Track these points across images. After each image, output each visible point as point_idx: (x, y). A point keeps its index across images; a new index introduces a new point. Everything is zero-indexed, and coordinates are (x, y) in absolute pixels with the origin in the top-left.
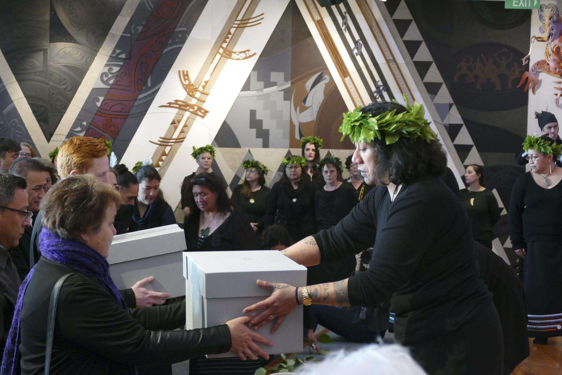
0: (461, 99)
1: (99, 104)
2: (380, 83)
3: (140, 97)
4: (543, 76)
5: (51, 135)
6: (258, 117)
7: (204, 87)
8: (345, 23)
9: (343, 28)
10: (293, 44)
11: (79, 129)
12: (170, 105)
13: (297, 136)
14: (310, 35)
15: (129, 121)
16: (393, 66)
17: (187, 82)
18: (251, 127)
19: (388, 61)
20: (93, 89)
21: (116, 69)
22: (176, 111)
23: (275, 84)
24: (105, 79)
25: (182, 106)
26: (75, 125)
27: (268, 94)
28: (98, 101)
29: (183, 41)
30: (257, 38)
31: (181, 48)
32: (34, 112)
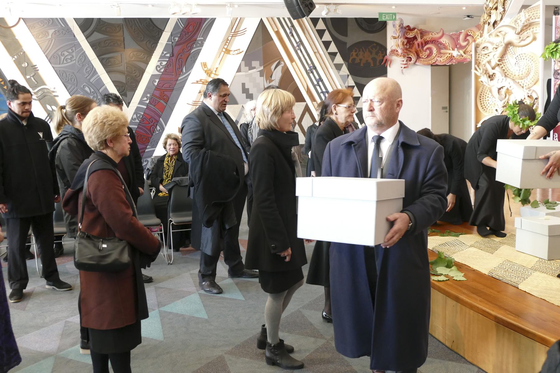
1: (156, 84)
2: (311, 65)
3: (180, 78)
4: (394, 58)
5: (129, 103)
6: (246, 87)
8: (291, 33)
9: (290, 35)
10: (263, 45)
11: (145, 99)
14: (272, 39)
15: (174, 92)
16: (318, 55)
17: (206, 69)
18: (243, 93)
19: (315, 53)
21: (164, 63)
23: (254, 68)
24: (159, 69)
26: (143, 97)
28: (155, 82)
29: (202, 45)
30: (242, 43)
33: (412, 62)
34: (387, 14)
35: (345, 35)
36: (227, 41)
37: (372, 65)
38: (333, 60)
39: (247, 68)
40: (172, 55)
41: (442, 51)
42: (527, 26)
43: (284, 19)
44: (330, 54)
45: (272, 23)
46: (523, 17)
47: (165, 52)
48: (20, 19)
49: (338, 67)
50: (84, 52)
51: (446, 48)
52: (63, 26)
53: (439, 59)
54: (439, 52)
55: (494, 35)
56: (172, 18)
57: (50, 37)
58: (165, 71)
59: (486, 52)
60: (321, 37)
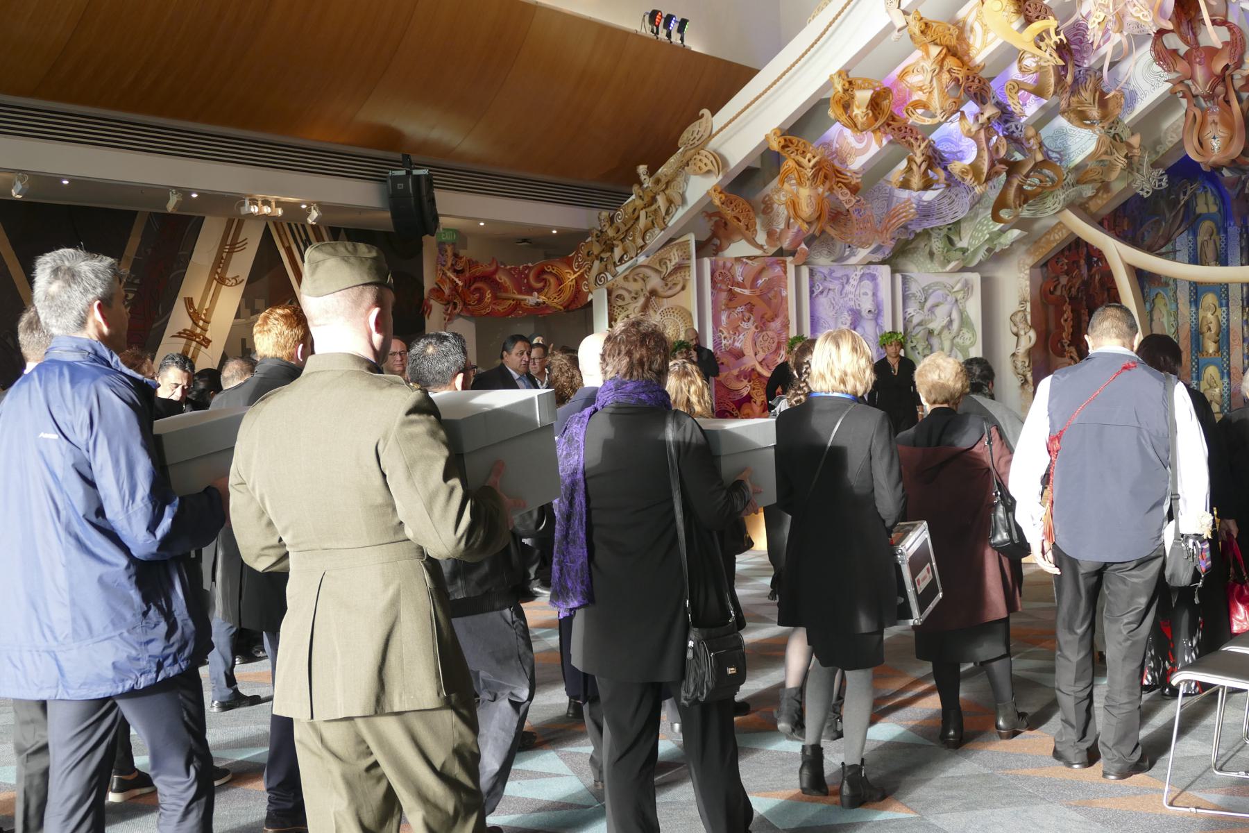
12: (179, 335)
21: (131, 296)
22: (184, 341)
25: (189, 335)
30: (243, 263)
33: (458, 310)
42: (680, 268)
46: (675, 258)
53: (496, 308)
54: (495, 297)
55: (630, 278)
59: (620, 303)
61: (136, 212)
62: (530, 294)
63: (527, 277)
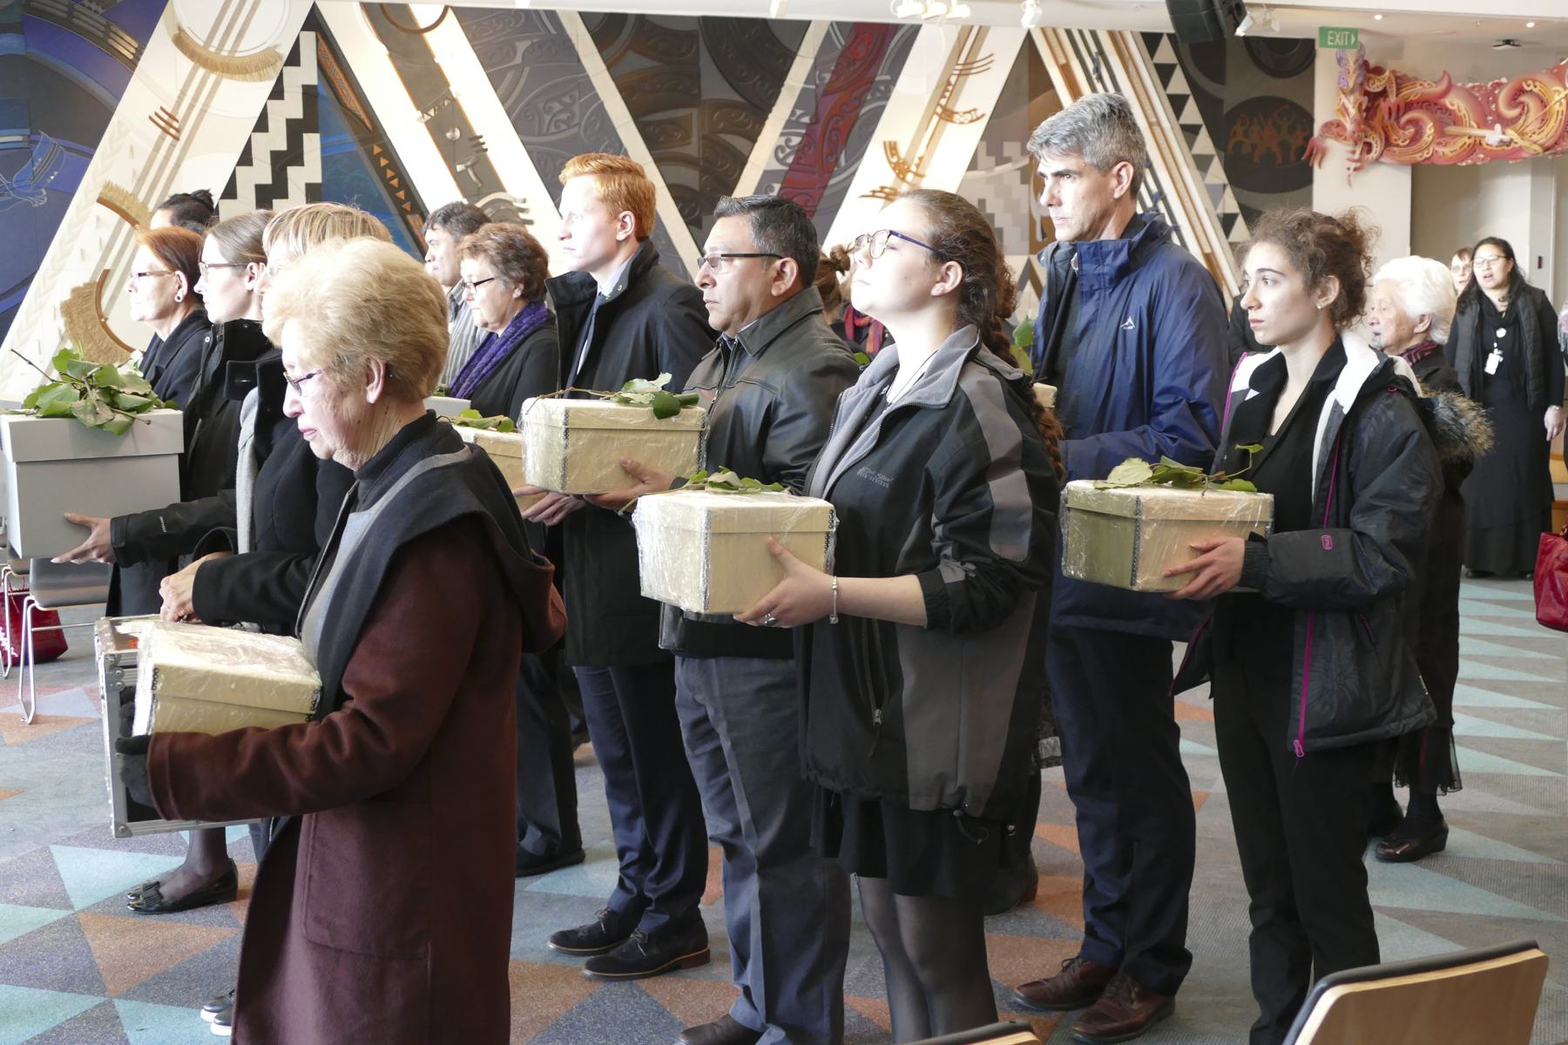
0: (1238, 175)
3: (832, 182)
4: (1330, 143)
7: (918, 166)
8: (1097, 70)
9: (1094, 77)
12: (874, 194)
13: (1039, 237)
14: (1050, 86)
16: (1157, 129)
19: (1150, 125)
20: (766, 172)
21: (796, 141)
23: (1008, 160)
24: (781, 156)
27: (1000, 176)
29: (886, 96)
30: (983, 92)
31: (884, 107)
32: (681, 211)
33: (1373, 155)
34: (1338, 30)
35: (1219, 78)
36: (947, 89)
37: (1280, 161)
38: (1190, 144)
39: (992, 159)
40: (815, 119)
41: (1452, 129)
43: (1081, 32)
44: (1185, 128)
45: (1055, 43)
47: (799, 112)
48: (446, 8)
49: (1202, 163)
50: (602, 104)
51: (1457, 121)
52: (553, 31)
53: (1441, 150)
54: (1440, 132)
56: (820, 23)
57: (518, 60)
58: (796, 161)
60: (1165, 83)
61: (808, 23)
62: (1490, 126)
63: (1495, 101)
